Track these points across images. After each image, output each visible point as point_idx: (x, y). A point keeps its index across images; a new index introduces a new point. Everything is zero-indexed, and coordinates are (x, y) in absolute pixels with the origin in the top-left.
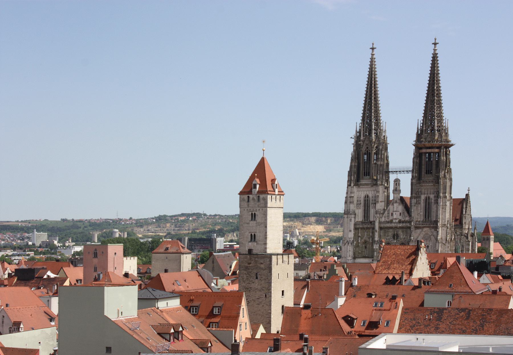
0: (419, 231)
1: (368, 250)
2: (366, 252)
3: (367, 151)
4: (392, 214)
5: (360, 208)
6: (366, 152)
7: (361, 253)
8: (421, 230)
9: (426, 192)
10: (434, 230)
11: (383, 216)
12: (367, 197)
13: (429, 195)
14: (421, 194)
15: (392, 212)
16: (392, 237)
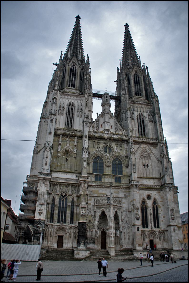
0: (136, 147)
1: (69, 163)
2: (66, 165)
3: (73, 68)
4: (101, 125)
5: (62, 115)
6: (72, 69)
7: (60, 166)
8: (138, 146)
9: (139, 110)
10: (152, 147)
11: (92, 126)
12: (71, 105)
13: (142, 113)
14: (134, 111)
15: (102, 124)
16: (103, 150)
